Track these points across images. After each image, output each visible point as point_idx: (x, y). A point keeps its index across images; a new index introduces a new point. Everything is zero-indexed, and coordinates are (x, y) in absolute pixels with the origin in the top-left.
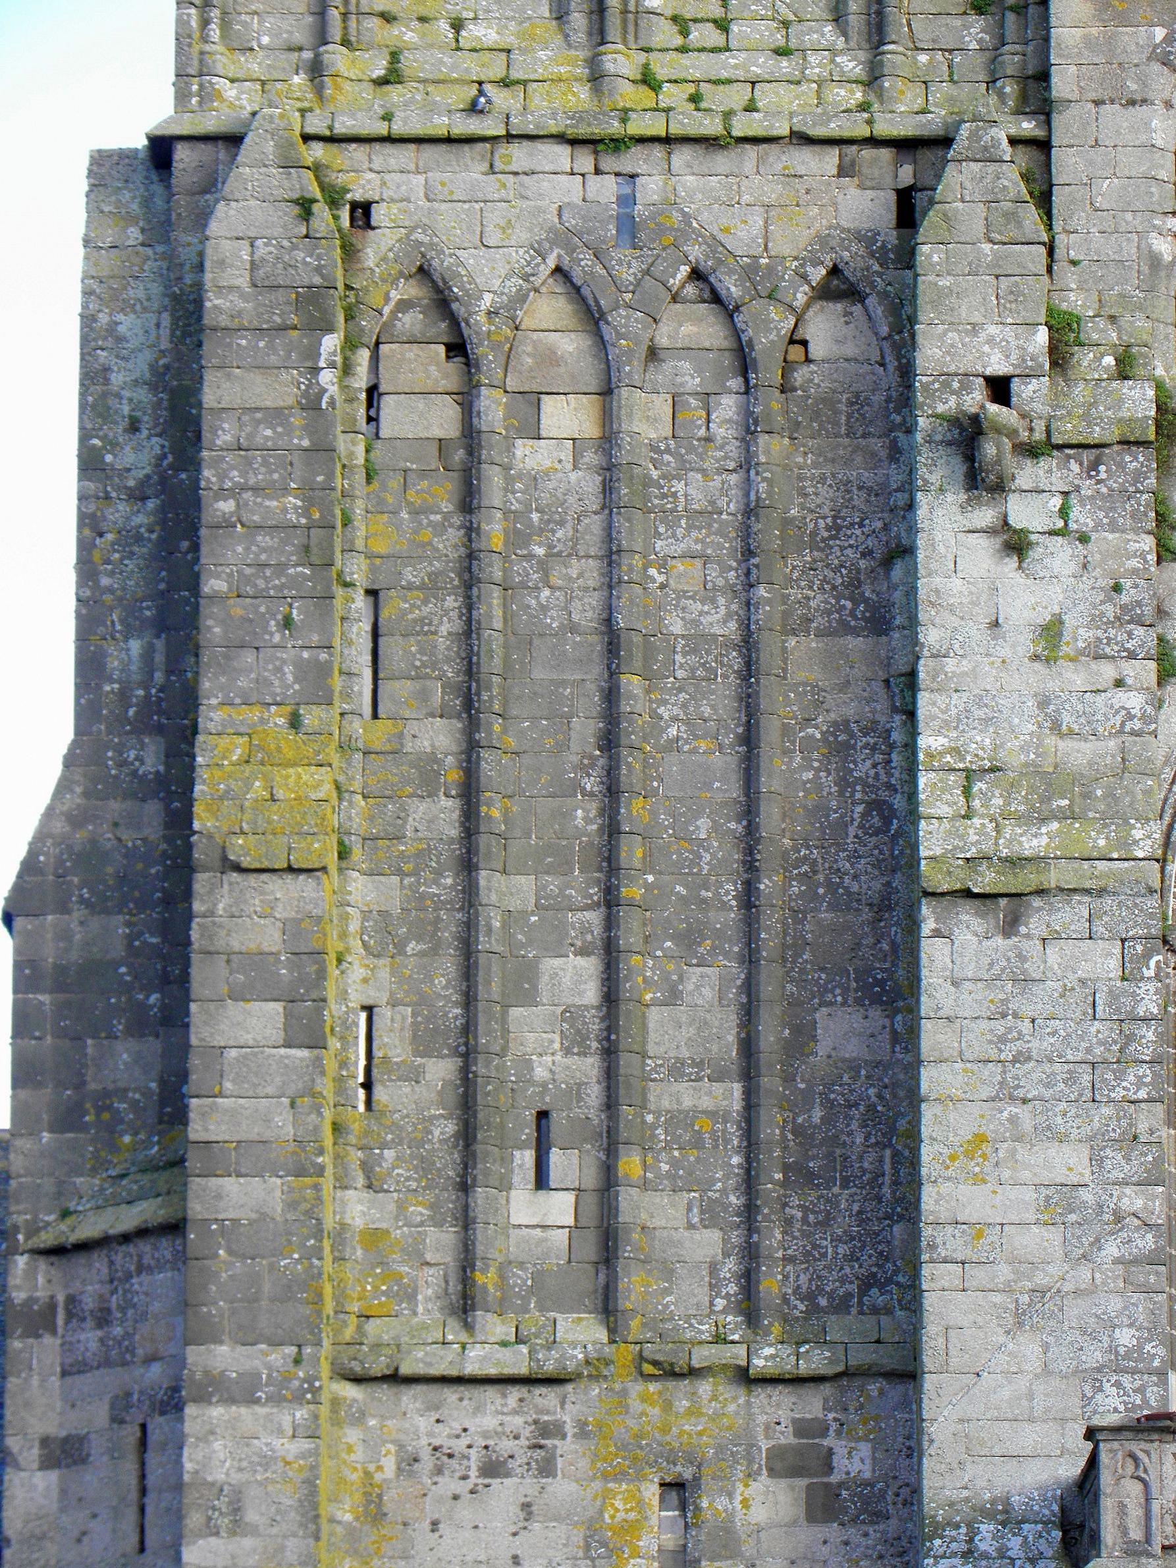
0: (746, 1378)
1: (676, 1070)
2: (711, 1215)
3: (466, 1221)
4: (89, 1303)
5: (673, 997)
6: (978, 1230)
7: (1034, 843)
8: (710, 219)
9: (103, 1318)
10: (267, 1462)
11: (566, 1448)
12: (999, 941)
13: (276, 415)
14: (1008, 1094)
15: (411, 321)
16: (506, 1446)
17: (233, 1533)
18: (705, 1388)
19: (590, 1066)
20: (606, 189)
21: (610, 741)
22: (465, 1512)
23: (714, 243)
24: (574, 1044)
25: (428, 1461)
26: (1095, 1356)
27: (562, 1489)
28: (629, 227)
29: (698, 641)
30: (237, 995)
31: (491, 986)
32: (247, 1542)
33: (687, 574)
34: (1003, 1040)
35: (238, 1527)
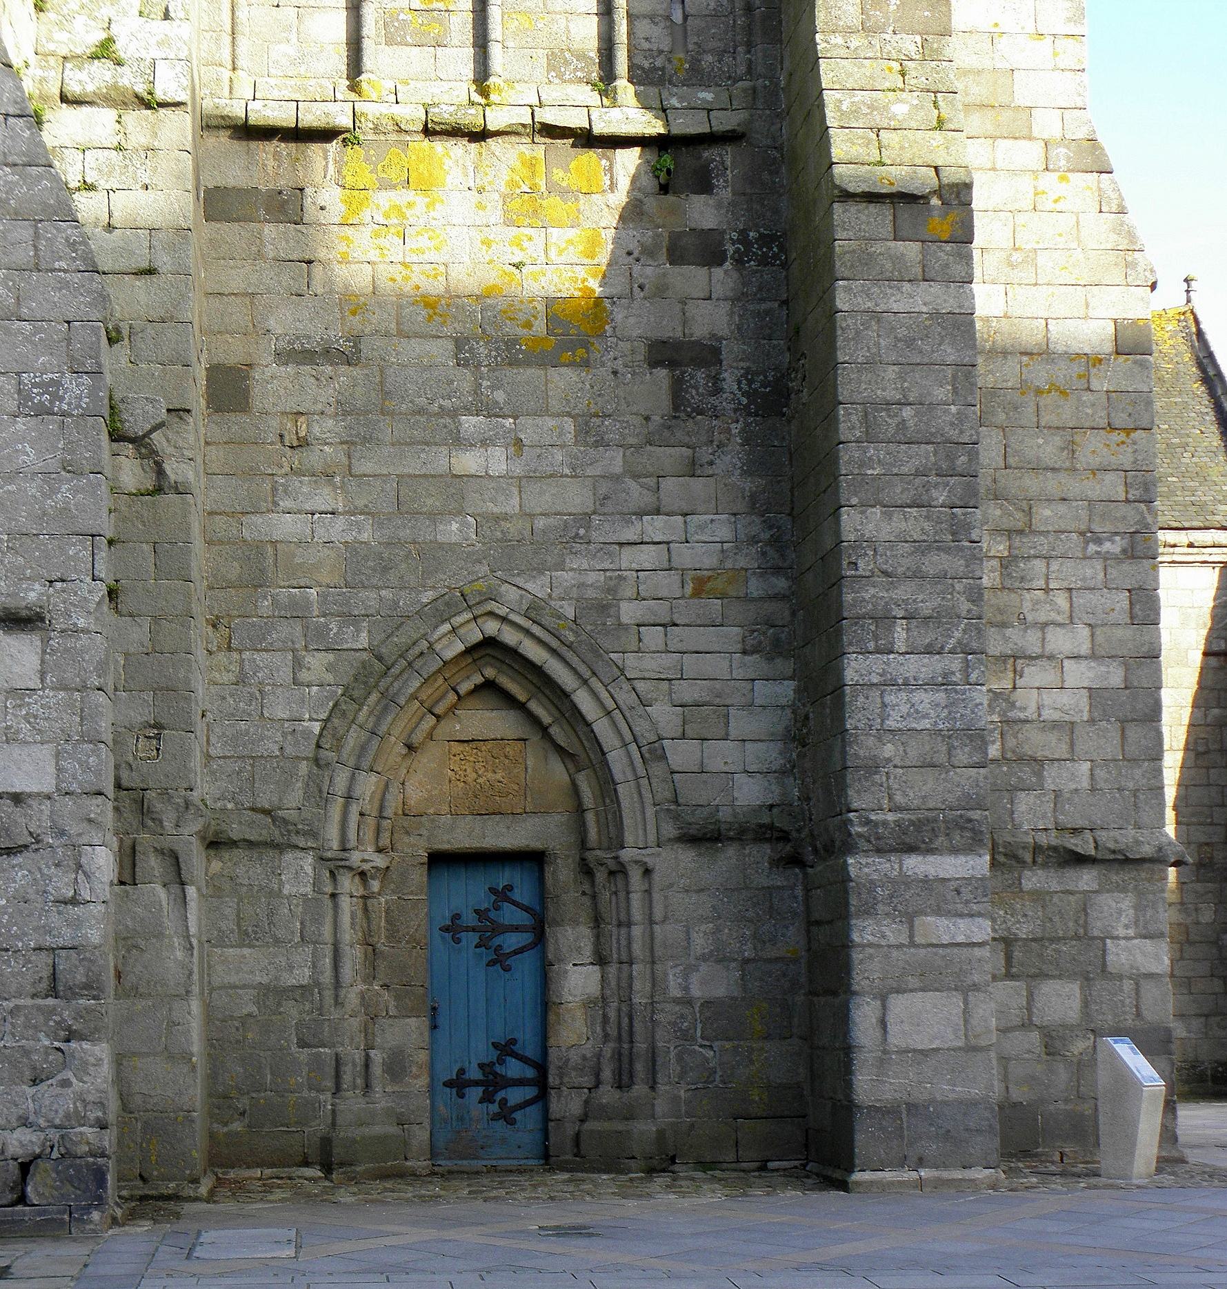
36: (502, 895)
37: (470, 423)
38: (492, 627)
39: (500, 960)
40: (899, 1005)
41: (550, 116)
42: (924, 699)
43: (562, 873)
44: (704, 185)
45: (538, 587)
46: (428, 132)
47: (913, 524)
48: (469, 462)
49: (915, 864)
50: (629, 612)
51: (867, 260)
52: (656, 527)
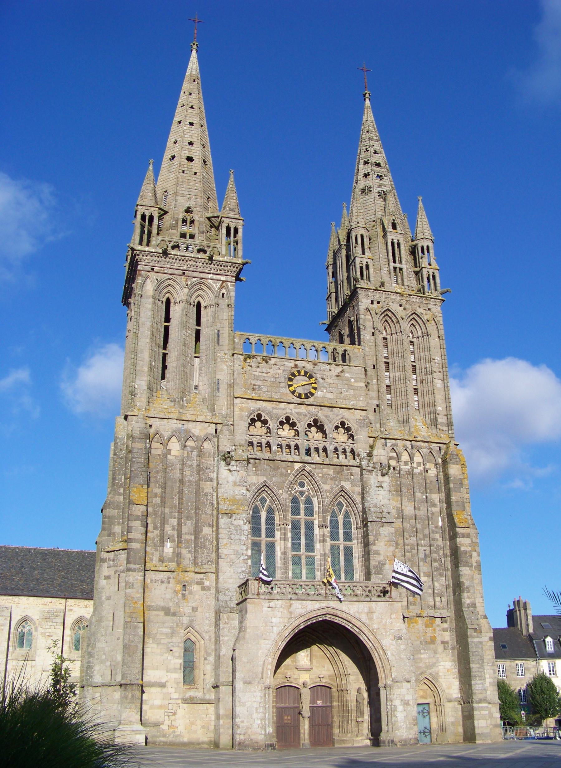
2: (190, 552)
4: (112, 559)
6: (226, 555)
8: (193, 431)
9: (113, 561)
10: (137, 579)
11: (171, 580)
12: (230, 520)
13: (141, 449)
16: (164, 579)
17: (132, 588)
18: (189, 573)
19: (175, 533)
23: (193, 434)
24: (173, 529)
25: (154, 581)
26: (240, 571)
27: (171, 585)
29: (189, 481)
30: (135, 520)
32: (134, 590)
34: (229, 532)
36: (424, 709)
37: (422, 651)
38: (426, 676)
39: (424, 717)
40: (480, 721)
41: (429, 615)
42: (480, 686)
43: (432, 706)
44: (446, 622)
45: (430, 671)
46: (417, 617)
47: (478, 665)
48: (422, 656)
49: (481, 705)
50: (440, 674)
51: (471, 636)
52: (442, 663)
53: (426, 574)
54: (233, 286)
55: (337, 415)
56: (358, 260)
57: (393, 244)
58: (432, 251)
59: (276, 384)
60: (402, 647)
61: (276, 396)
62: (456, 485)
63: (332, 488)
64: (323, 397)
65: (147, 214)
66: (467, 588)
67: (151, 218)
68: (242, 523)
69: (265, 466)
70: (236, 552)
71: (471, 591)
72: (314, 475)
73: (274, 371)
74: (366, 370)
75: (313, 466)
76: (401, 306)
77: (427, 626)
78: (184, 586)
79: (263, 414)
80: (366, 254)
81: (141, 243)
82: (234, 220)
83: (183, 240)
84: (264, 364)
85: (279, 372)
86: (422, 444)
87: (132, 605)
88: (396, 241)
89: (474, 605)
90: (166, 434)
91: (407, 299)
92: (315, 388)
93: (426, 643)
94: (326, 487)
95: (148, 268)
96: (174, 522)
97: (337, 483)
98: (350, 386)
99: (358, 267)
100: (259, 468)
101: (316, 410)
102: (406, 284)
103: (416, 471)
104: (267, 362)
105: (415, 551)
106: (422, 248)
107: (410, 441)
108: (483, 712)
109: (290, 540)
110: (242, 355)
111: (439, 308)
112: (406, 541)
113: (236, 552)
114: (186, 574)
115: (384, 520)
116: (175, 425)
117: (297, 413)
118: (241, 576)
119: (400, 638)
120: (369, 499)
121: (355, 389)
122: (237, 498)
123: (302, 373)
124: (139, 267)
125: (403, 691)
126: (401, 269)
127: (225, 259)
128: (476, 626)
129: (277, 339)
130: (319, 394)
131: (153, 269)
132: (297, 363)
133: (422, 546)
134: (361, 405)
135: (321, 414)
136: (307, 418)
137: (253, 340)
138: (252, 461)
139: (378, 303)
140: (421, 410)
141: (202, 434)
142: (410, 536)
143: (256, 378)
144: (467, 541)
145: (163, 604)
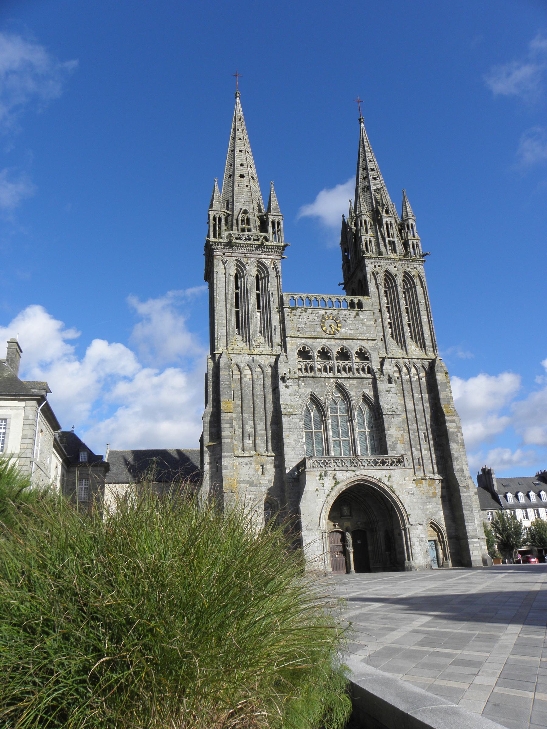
0: (268, 456)
1: (260, 430)
3: (243, 443)
5: (259, 424)
7: (291, 410)
8: (260, 361)
11: (253, 463)
13: (226, 375)
14: (290, 431)
15: (235, 369)
19: (253, 430)
20: (251, 358)
21: (253, 403)
22: (245, 468)
27: (252, 466)
28: (253, 361)
29: (260, 395)
31: (244, 423)
33: (259, 389)
35: (227, 469)
47: (469, 512)
48: (428, 507)
49: (473, 540)
53: (425, 450)
54: (279, 262)
55: (357, 344)
56: (363, 238)
57: (387, 224)
58: (415, 228)
59: (313, 327)
60: (415, 500)
61: (314, 334)
62: (442, 387)
63: (356, 394)
64: (346, 333)
65: (217, 217)
66: (456, 458)
67: (220, 219)
68: (297, 420)
69: (311, 381)
70: (295, 440)
71: (460, 460)
72: (344, 385)
73: (312, 317)
74: (374, 313)
75: (343, 379)
76: (395, 267)
77: (429, 485)
78: (262, 466)
79: (307, 347)
80: (369, 233)
81: (215, 236)
82: (276, 217)
83: (243, 233)
84: (304, 313)
85: (315, 318)
86: (416, 360)
87: (227, 481)
88: (389, 222)
89: (462, 470)
90: (242, 365)
91: (399, 262)
92: (340, 327)
93: (430, 497)
94: (352, 393)
95: (221, 254)
96: (252, 422)
97: (360, 390)
98: (364, 324)
99: (364, 242)
100: (307, 383)
101: (342, 342)
102: (398, 251)
103: (413, 379)
104: (306, 312)
105: (417, 434)
106: (408, 226)
107: (408, 359)
108: (475, 545)
109: (331, 430)
110: (289, 308)
111: (422, 267)
112: (410, 427)
113: (295, 440)
114: (262, 457)
115: (394, 413)
116: (248, 358)
117: (329, 345)
118: (300, 457)
119: (412, 494)
120: (382, 400)
121: (367, 326)
122: (293, 404)
123: (331, 318)
124: (215, 253)
125: (418, 532)
126: (394, 242)
127: (272, 244)
128: (465, 485)
129: (312, 296)
130: (343, 331)
131: (224, 254)
132: (327, 311)
133: (421, 430)
134: (372, 336)
135: (346, 343)
136: (336, 347)
137: (297, 297)
138: (301, 379)
139: (379, 266)
140: (414, 338)
141: (267, 363)
142: (413, 424)
143: (300, 323)
144: (454, 425)
145: (248, 479)
